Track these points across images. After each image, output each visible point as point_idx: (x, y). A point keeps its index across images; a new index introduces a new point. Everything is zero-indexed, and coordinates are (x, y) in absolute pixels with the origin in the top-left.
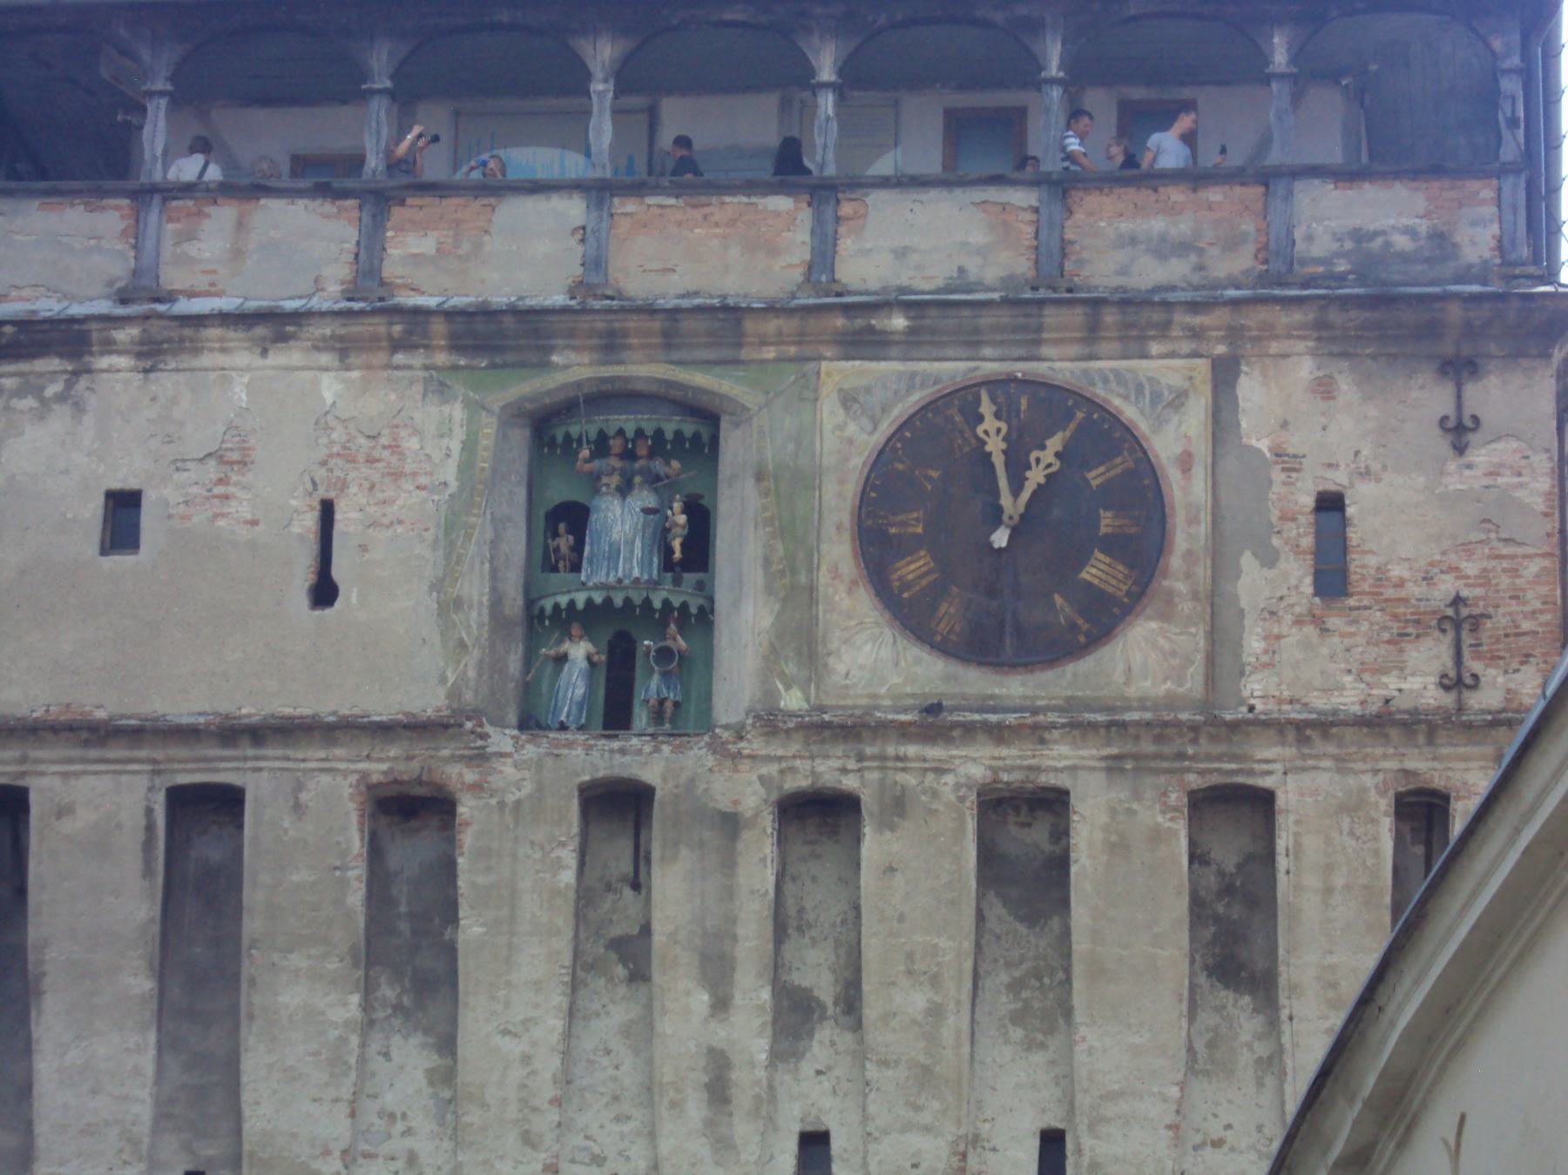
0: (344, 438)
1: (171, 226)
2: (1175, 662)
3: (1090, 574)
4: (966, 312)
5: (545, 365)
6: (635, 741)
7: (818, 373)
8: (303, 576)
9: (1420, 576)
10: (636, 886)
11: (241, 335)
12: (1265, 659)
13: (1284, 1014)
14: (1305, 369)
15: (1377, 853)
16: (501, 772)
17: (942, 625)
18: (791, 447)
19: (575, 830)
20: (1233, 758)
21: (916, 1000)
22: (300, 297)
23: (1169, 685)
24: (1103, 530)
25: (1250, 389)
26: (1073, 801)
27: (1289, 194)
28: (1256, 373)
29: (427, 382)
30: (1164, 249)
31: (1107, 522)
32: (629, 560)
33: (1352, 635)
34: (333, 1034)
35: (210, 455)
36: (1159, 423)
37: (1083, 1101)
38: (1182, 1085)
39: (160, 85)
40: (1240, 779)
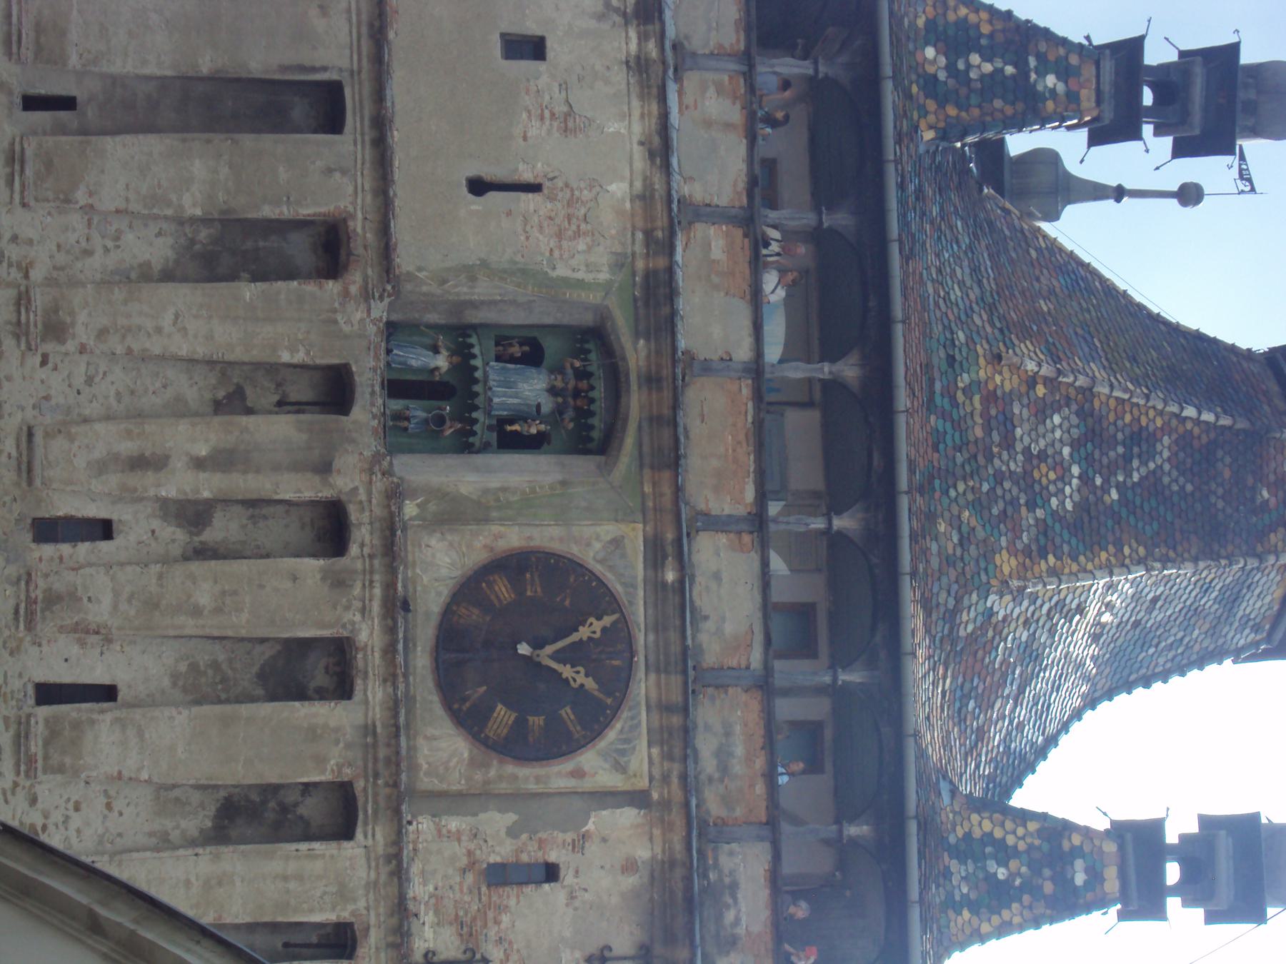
0: (583, 198)
1: (726, 78)
2: (441, 770)
3: (500, 709)
4: (678, 622)
5: (637, 335)
6: (380, 401)
7: (635, 522)
8: (489, 172)
9: (503, 935)
10: (280, 404)
11: (653, 127)
12: (444, 831)
13: (200, 851)
14: (643, 853)
15: (311, 911)
16: (357, 310)
17: (463, 610)
18: (584, 504)
19: (319, 361)
20: (375, 812)
21: (204, 597)
22: (680, 167)
23: (425, 766)
24: (530, 719)
25: (628, 816)
26: (344, 702)
27: (761, 839)
28: (640, 820)
29: (625, 255)
30: (723, 755)
32: (505, 395)
33: (461, 891)
34: (174, 198)
35: (571, 106)
36: (604, 755)
37: (137, 714)
38: (148, 782)
39: (822, 69)
40: (361, 816)
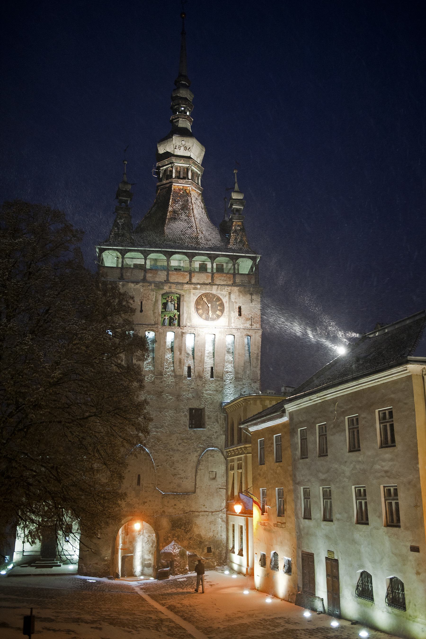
5: (163, 289)
31: (219, 308)
37: (215, 364)
